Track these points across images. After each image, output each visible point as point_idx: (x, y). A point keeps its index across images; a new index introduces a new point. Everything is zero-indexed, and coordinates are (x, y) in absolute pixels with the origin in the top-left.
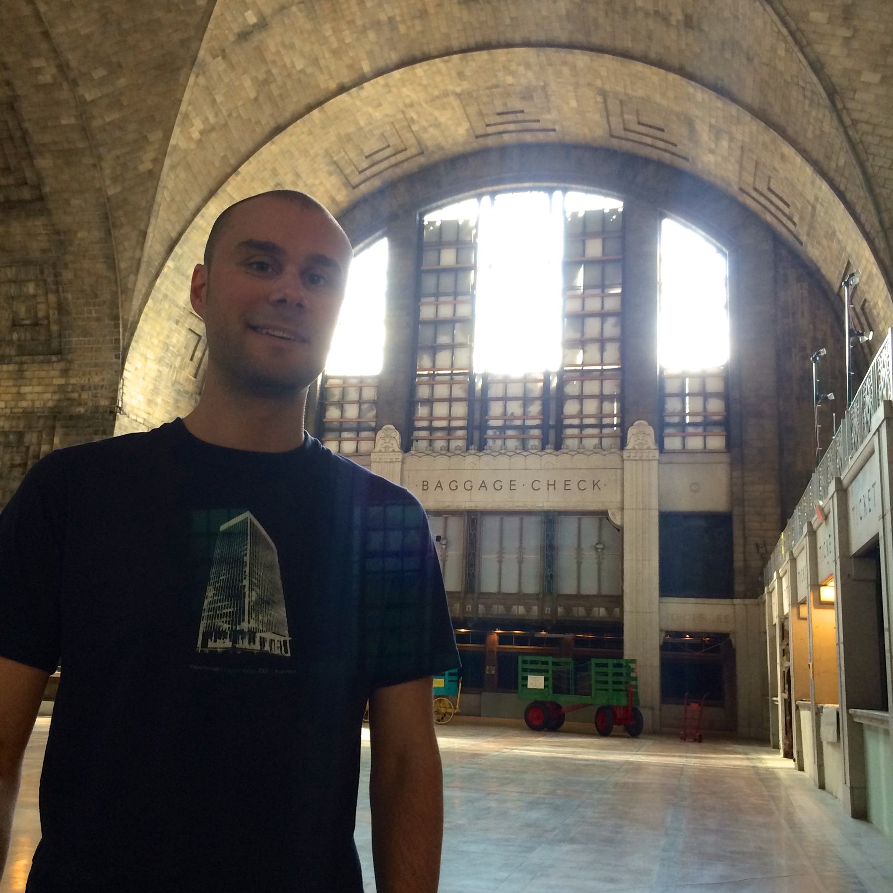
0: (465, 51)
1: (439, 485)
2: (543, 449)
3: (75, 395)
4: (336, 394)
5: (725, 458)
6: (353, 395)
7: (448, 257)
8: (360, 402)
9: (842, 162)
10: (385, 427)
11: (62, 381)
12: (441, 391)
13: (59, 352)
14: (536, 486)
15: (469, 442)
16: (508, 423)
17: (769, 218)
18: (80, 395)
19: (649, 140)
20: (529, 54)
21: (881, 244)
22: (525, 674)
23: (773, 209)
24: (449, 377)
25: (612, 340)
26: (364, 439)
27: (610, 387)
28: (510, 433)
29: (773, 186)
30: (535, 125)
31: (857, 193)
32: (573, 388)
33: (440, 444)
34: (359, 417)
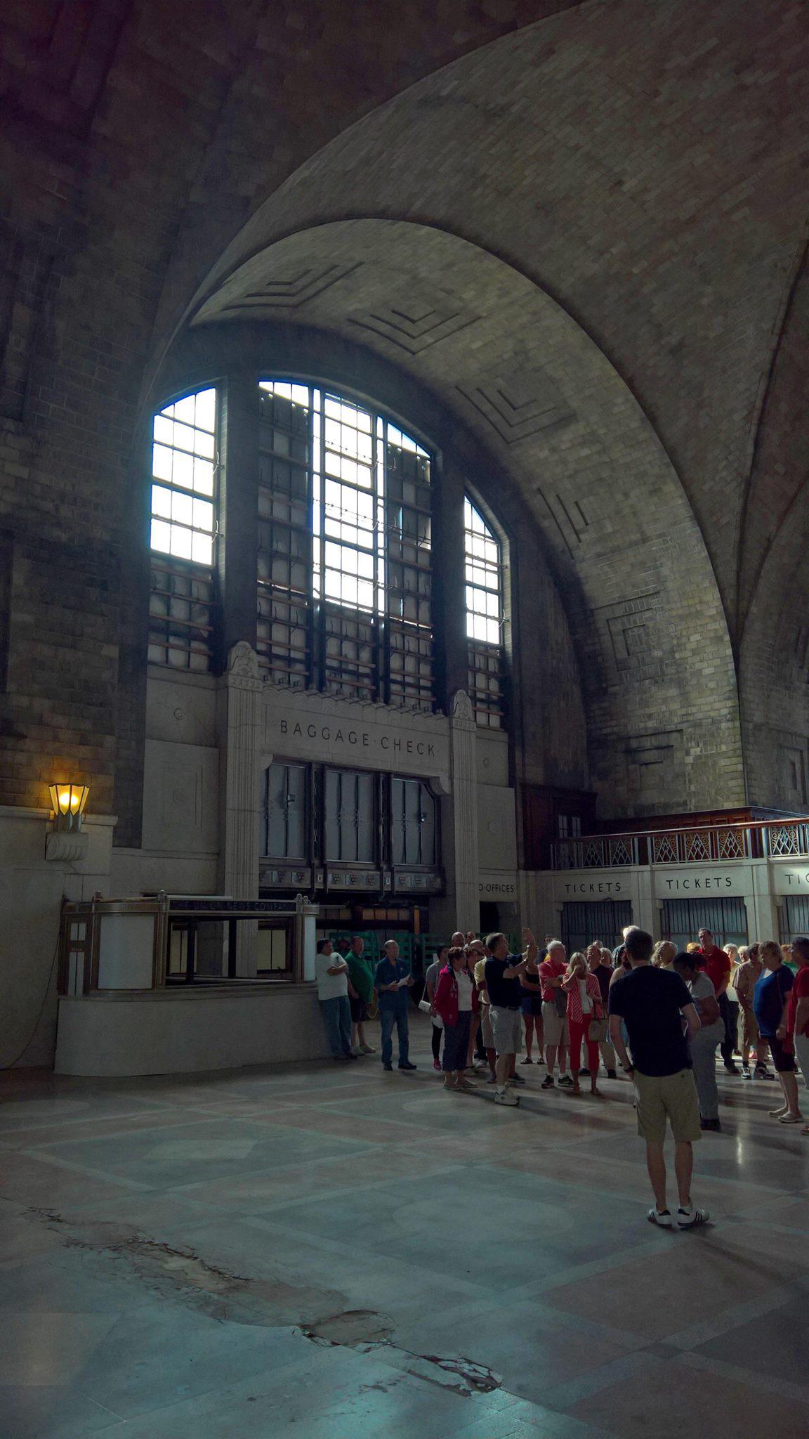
0: (488, 249)
1: (298, 729)
2: (434, 712)
3: (48, 506)
4: (160, 578)
5: (504, 737)
6: (180, 588)
7: (280, 445)
8: (190, 601)
9: (724, 521)
10: (240, 643)
11: (24, 473)
12: (280, 611)
13: (19, 418)
14: (386, 743)
15: (308, 680)
16: (344, 666)
17: (547, 524)
18: (57, 509)
19: (487, 408)
20: (526, 284)
21: (731, 594)
22: (429, 952)
23: (562, 518)
24: (285, 596)
25: (425, 597)
26: (173, 647)
27: (424, 648)
28: (345, 677)
29: (584, 503)
30: (404, 339)
31: (727, 550)
32: (395, 640)
33: (278, 675)
34: (190, 620)
